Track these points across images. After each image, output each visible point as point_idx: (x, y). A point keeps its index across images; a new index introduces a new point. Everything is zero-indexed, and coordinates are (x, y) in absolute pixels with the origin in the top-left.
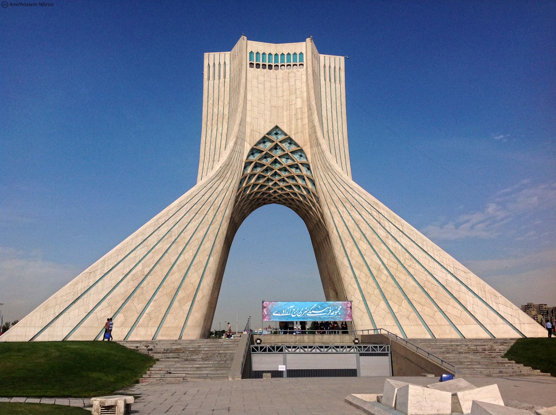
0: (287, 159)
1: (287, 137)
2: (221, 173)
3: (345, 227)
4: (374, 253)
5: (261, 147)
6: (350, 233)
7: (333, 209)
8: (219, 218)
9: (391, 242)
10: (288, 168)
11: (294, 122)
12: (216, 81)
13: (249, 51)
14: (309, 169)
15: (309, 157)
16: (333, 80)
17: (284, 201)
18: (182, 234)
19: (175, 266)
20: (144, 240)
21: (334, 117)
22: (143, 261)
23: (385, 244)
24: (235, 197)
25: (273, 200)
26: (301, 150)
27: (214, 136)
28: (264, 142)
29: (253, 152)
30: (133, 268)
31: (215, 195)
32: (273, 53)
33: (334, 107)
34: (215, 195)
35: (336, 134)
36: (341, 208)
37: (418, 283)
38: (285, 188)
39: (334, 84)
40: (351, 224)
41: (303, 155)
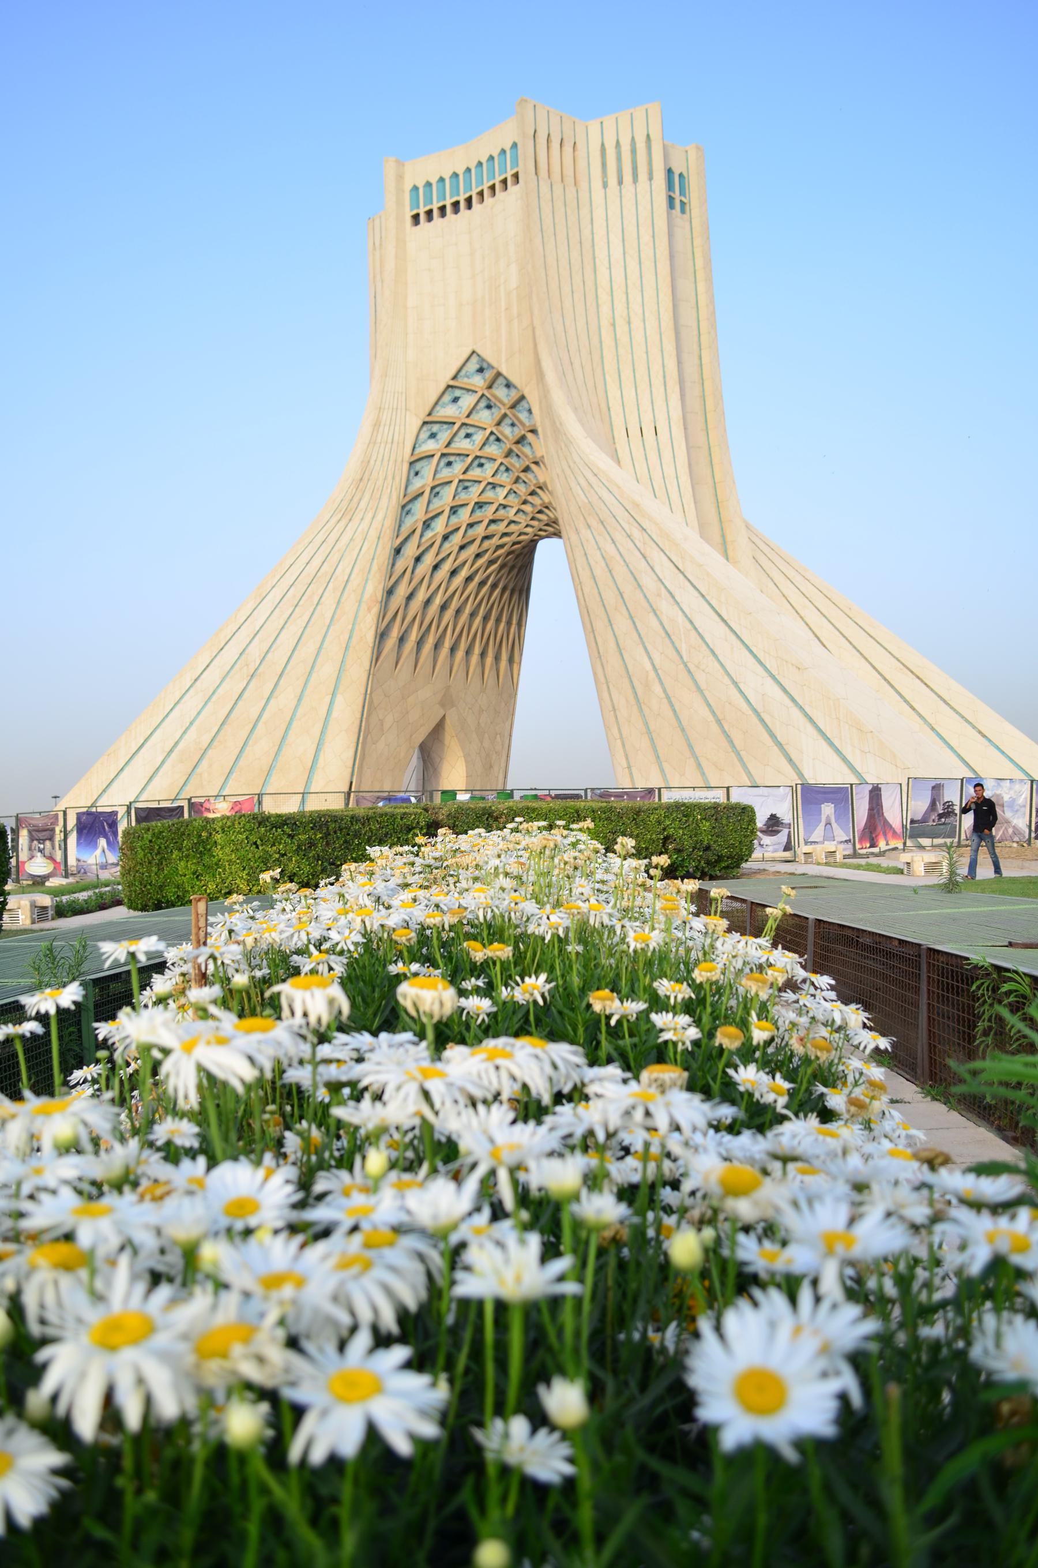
2: (345, 503)
5: (448, 411)
6: (600, 593)
9: (665, 607)
13: (408, 187)
15: (535, 410)
16: (628, 177)
18: (269, 655)
19: (260, 725)
22: (196, 723)
23: (656, 614)
28: (456, 400)
31: (335, 557)
32: (460, 171)
34: (335, 557)
35: (637, 323)
37: (713, 713)
39: (631, 188)
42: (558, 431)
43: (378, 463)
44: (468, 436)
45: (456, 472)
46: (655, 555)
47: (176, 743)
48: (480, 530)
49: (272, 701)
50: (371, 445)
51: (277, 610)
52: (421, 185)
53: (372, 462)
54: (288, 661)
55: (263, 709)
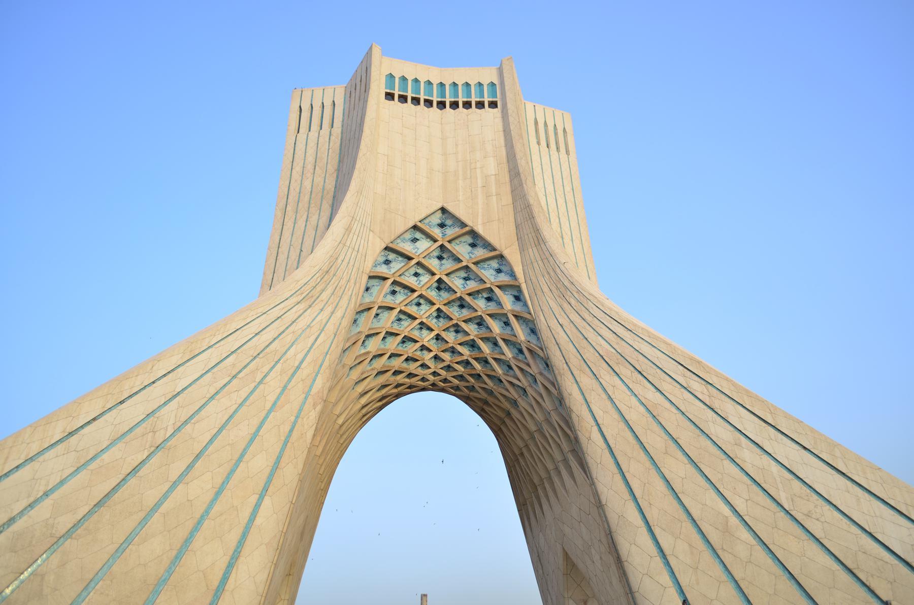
1: (467, 229)
2: (307, 288)
3: (622, 425)
4: (708, 486)
7: (586, 381)
9: (748, 456)
10: (468, 299)
11: (481, 200)
12: (313, 134)
15: (518, 270)
17: (456, 382)
20: (71, 434)
21: (562, 209)
22: (56, 495)
24: (339, 350)
25: (431, 378)
26: (501, 257)
27: (299, 232)
28: (415, 240)
30: (21, 513)
32: (435, 82)
33: (560, 192)
34: (288, 338)
38: (459, 348)
39: (556, 153)
40: (635, 414)
41: (503, 268)
42: (565, 289)
43: (345, 263)
44: (416, 275)
45: (398, 302)
46: (729, 410)
49: (180, 487)
50: (341, 245)
51: (209, 374)
52: (397, 76)
53: (339, 261)
54: (211, 441)
55: (165, 496)
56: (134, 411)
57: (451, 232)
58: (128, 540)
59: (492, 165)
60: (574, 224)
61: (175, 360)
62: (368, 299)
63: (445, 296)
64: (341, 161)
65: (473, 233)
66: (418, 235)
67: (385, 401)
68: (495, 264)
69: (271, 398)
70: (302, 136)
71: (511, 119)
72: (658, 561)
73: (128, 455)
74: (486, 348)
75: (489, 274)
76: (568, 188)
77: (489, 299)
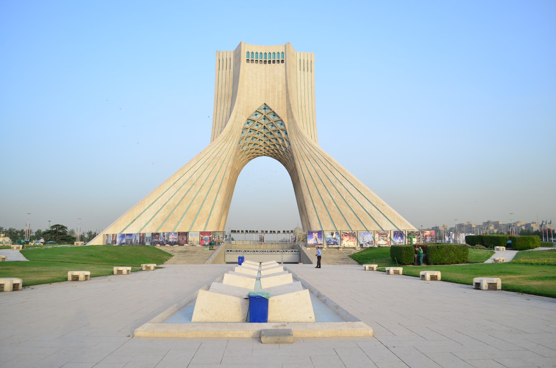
0: (272, 126)
5: (254, 118)
7: (301, 162)
8: (224, 167)
9: (338, 185)
10: (272, 132)
12: (224, 71)
14: (286, 133)
26: (282, 120)
28: (256, 115)
29: (249, 120)
32: (263, 53)
35: (307, 107)
36: (307, 162)
40: (313, 172)
42: (298, 133)
44: (257, 125)
47: (166, 203)
48: (252, 151)
52: (250, 52)
56: (187, 176)
57: (268, 111)
58: (190, 206)
59: (281, 87)
60: (310, 100)
61: (195, 163)
62: (243, 135)
63: (266, 131)
64: (233, 83)
65: (273, 112)
66: (257, 113)
67: (250, 160)
68: (280, 122)
69: (218, 169)
70: (221, 72)
71: (287, 70)
72: (314, 209)
73: (187, 187)
74: (278, 147)
75: (278, 125)
76: (310, 87)
77: (279, 133)
